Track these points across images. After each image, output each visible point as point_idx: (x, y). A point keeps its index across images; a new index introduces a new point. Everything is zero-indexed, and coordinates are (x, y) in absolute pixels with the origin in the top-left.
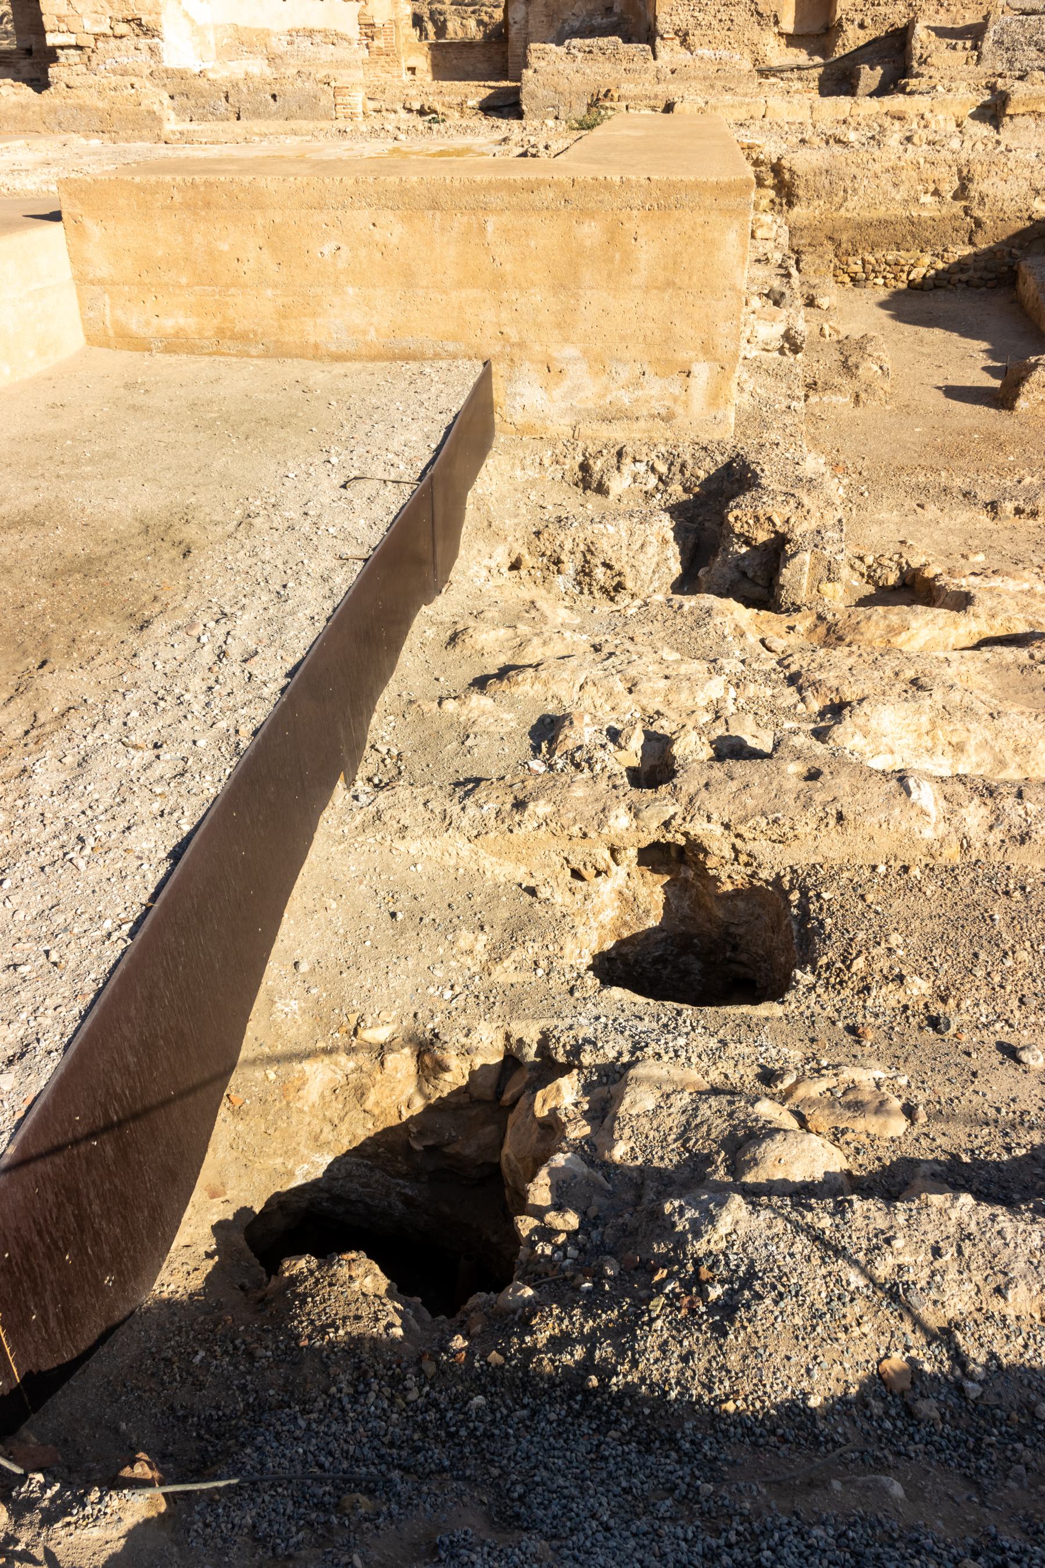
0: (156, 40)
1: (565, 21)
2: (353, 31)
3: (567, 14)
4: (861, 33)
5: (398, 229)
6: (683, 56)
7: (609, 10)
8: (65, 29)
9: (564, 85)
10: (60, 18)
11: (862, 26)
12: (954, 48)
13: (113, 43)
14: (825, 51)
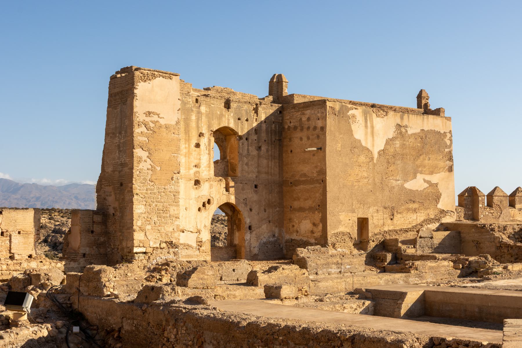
0: (177, 249)
1: (262, 239)
2: (194, 245)
3: (262, 237)
4: (373, 243)
6: (334, 251)
7: (274, 236)
8: (142, 245)
9: (319, 262)
10: (140, 241)
11: (373, 241)
12: (409, 247)
13: (159, 250)
14: (365, 250)
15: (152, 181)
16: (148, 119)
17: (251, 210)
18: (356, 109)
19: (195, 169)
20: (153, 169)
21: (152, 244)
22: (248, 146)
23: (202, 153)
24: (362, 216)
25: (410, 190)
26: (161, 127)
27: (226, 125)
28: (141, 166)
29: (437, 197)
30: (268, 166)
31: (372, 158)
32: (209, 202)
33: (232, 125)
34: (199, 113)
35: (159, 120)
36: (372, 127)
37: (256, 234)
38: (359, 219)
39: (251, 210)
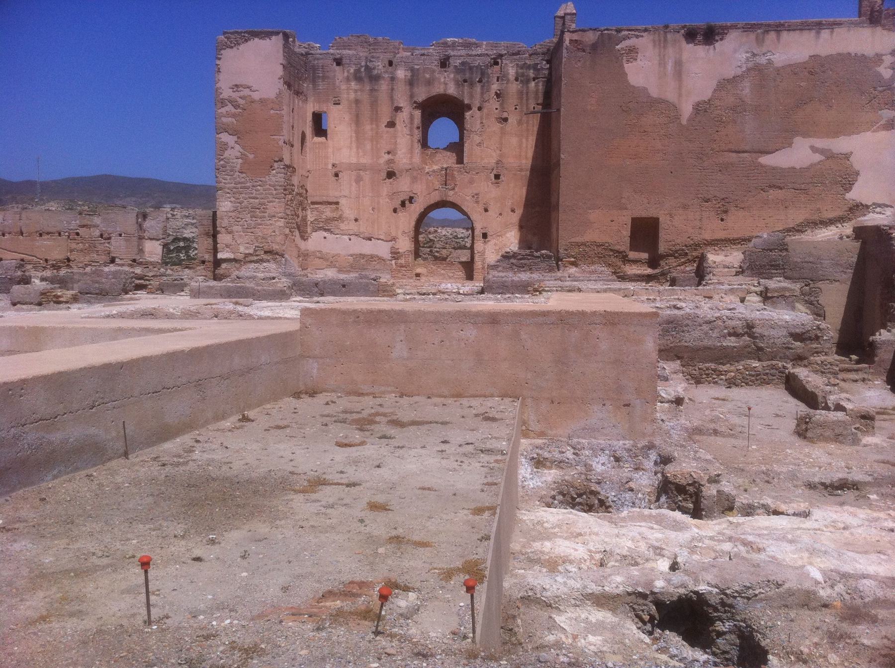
5: (474, 332)
10: (227, 246)
15: (241, 173)
16: (235, 95)
17: (486, 210)
18: (637, 37)
19: (387, 157)
20: (243, 156)
21: (242, 249)
22: (481, 118)
23: (400, 134)
24: (644, 214)
25: (774, 168)
26: (253, 102)
28: (227, 154)
29: (848, 179)
30: (520, 146)
31: (678, 117)
32: (411, 200)
33: (452, 90)
34: (393, 79)
35: (251, 93)
36: (679, 64)
37: (495, 244)
38: (634, 220)
39: (486, 210)
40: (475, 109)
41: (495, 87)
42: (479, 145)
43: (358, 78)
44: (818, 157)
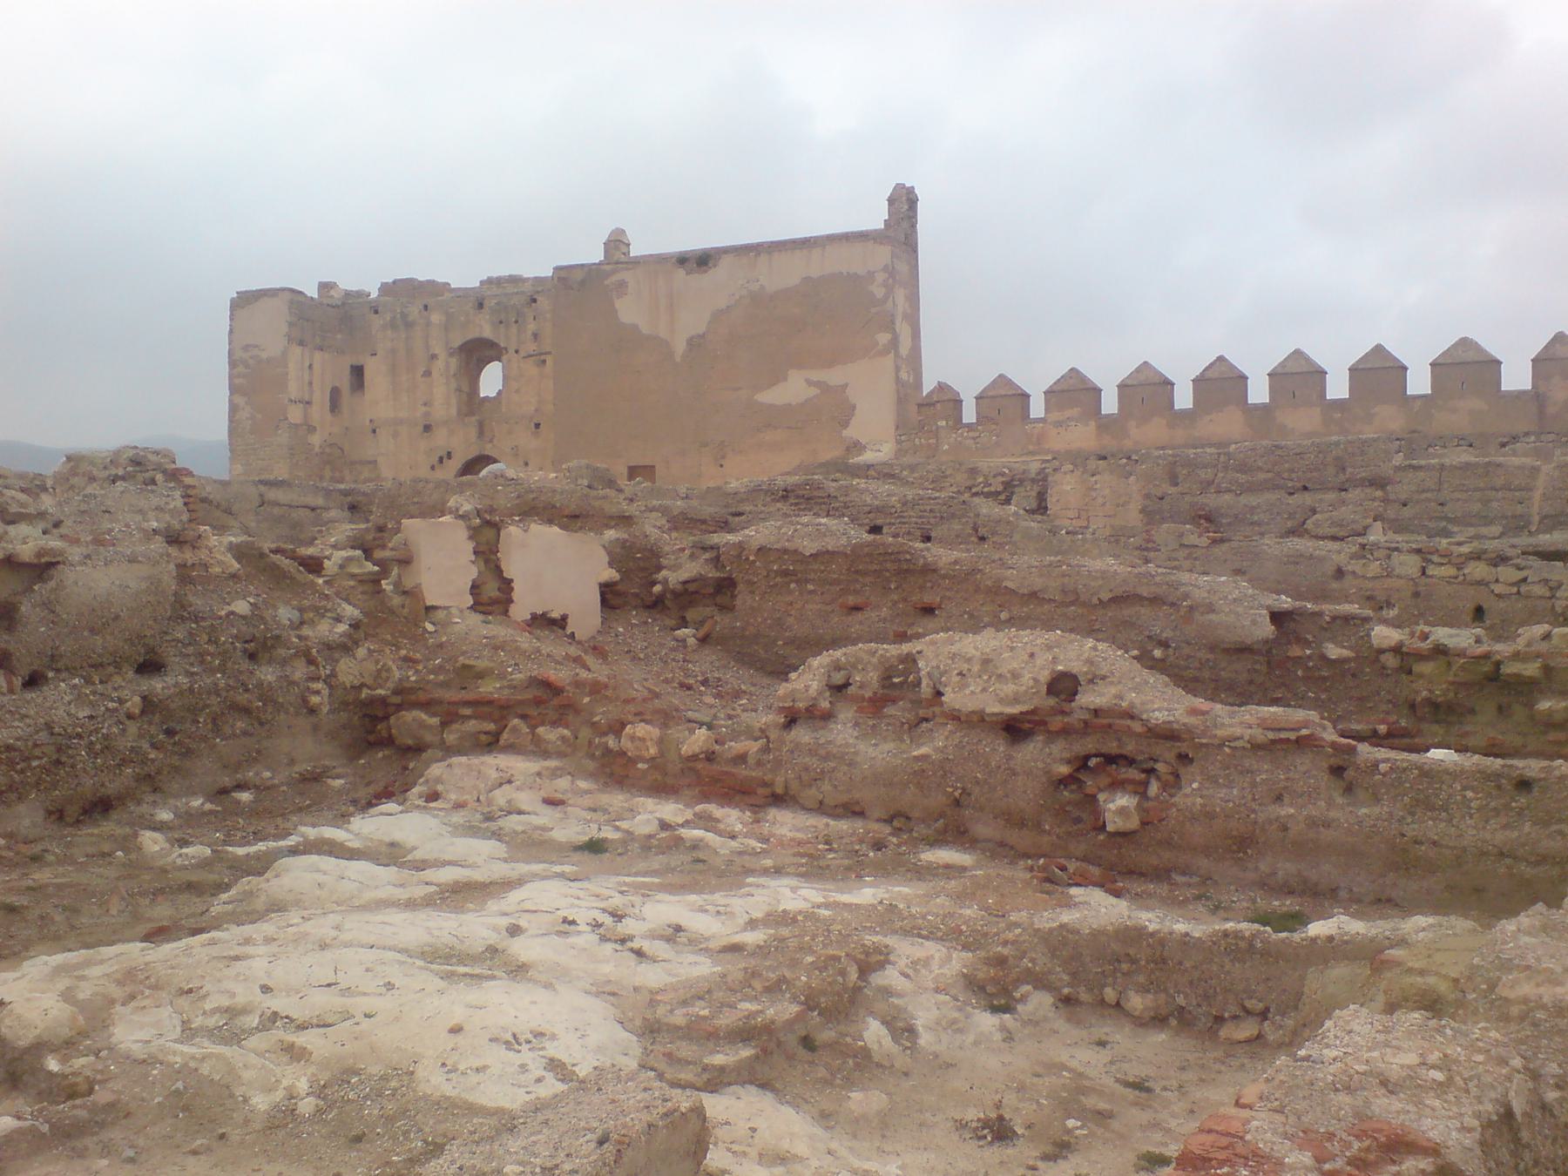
19: (424, 409)
27: (477, 335)
32: (449, 454)
33: (487, 333)
34: (428, 324)
40: (511, 351)
41: (531, 327)
42: (517, 391)
43: (393, 325)
44: (813, 391)
